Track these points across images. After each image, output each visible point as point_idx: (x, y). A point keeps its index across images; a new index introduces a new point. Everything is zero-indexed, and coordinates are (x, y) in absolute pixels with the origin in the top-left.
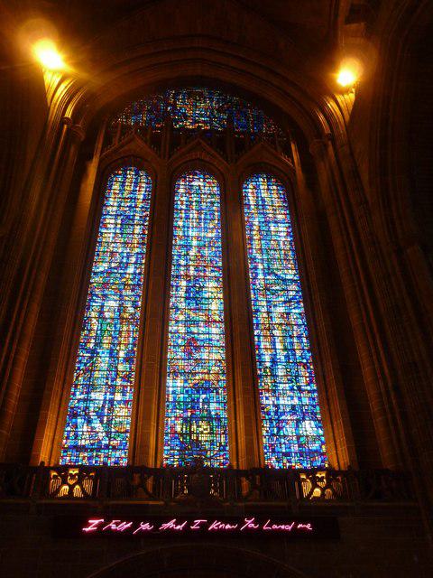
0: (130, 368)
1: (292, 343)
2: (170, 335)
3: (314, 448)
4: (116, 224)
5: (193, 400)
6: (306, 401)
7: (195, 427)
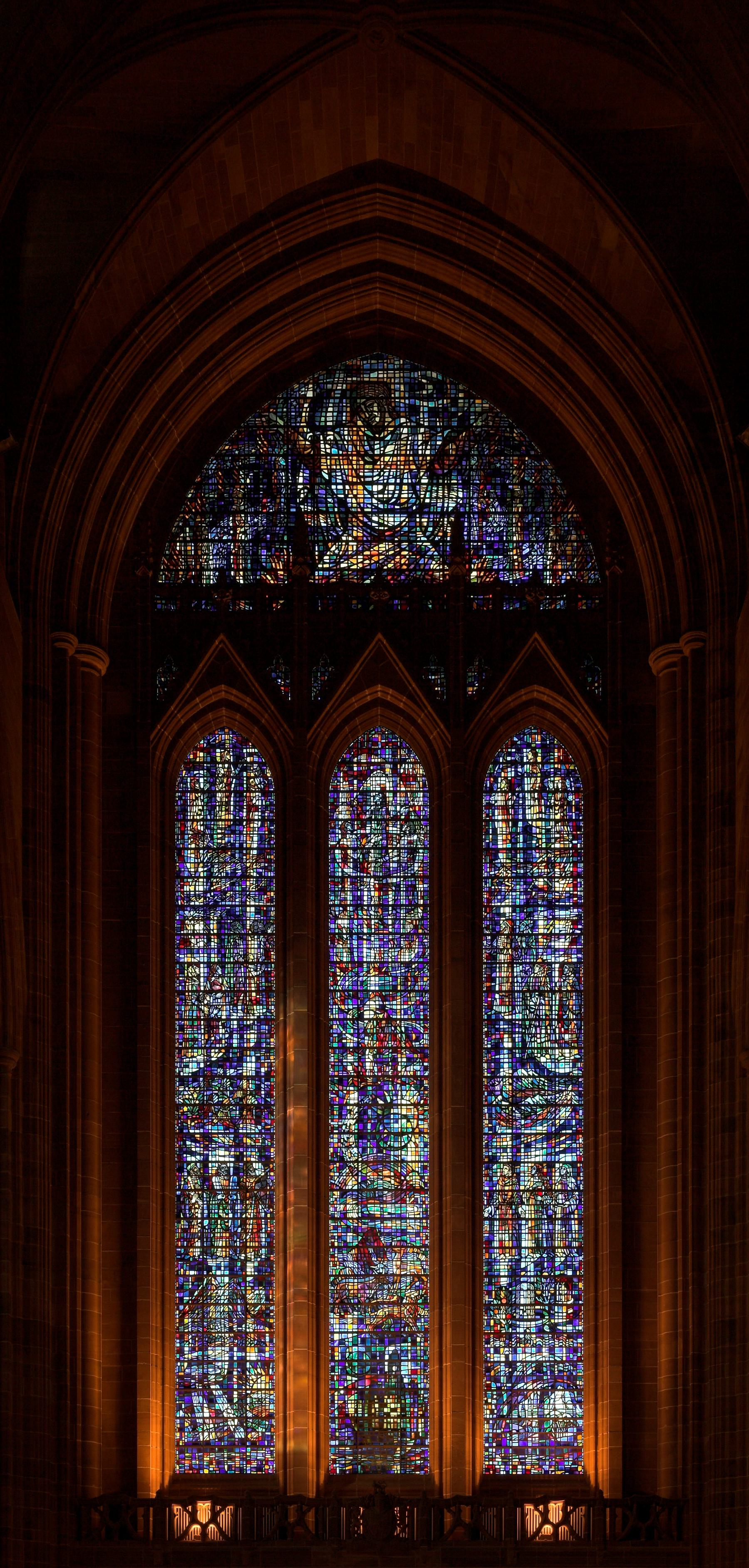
0: (267, 1299)
1: (551, 1235)
2: (332, 1224)
3: (565, 1439)
4: (208, 935)
5: (373, 1357)
6: (561, 1354)
7: (377, 1406)
